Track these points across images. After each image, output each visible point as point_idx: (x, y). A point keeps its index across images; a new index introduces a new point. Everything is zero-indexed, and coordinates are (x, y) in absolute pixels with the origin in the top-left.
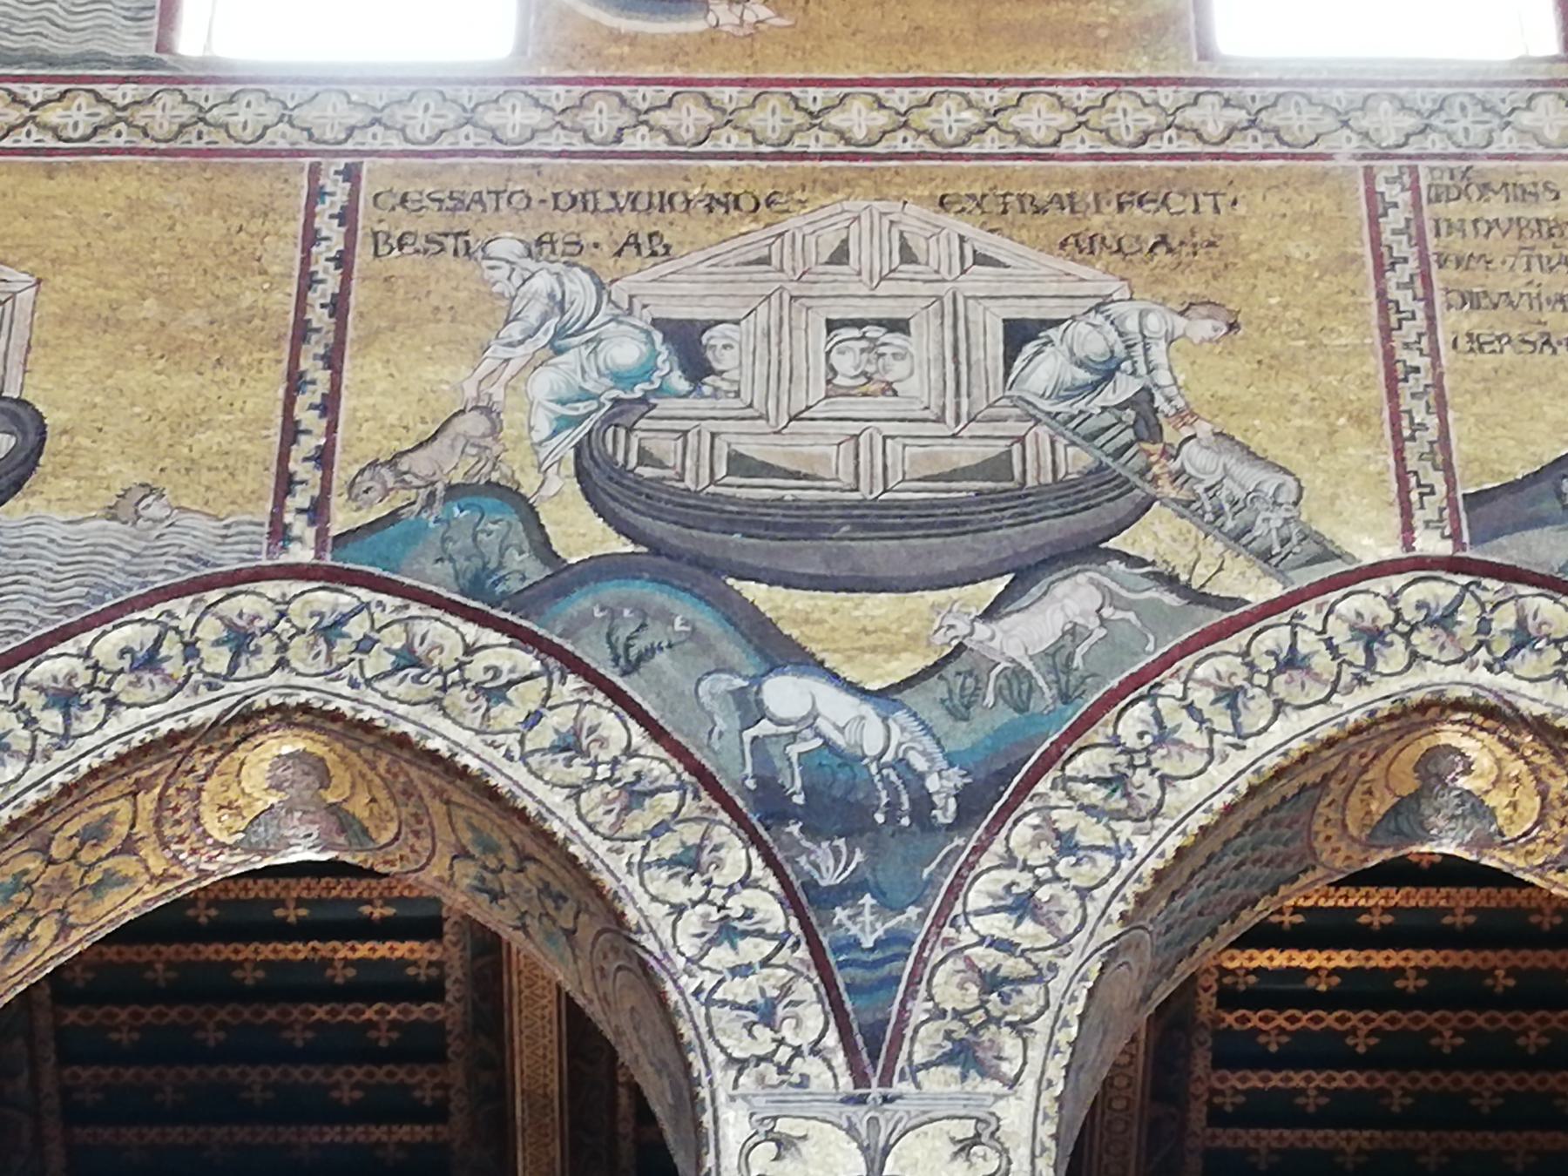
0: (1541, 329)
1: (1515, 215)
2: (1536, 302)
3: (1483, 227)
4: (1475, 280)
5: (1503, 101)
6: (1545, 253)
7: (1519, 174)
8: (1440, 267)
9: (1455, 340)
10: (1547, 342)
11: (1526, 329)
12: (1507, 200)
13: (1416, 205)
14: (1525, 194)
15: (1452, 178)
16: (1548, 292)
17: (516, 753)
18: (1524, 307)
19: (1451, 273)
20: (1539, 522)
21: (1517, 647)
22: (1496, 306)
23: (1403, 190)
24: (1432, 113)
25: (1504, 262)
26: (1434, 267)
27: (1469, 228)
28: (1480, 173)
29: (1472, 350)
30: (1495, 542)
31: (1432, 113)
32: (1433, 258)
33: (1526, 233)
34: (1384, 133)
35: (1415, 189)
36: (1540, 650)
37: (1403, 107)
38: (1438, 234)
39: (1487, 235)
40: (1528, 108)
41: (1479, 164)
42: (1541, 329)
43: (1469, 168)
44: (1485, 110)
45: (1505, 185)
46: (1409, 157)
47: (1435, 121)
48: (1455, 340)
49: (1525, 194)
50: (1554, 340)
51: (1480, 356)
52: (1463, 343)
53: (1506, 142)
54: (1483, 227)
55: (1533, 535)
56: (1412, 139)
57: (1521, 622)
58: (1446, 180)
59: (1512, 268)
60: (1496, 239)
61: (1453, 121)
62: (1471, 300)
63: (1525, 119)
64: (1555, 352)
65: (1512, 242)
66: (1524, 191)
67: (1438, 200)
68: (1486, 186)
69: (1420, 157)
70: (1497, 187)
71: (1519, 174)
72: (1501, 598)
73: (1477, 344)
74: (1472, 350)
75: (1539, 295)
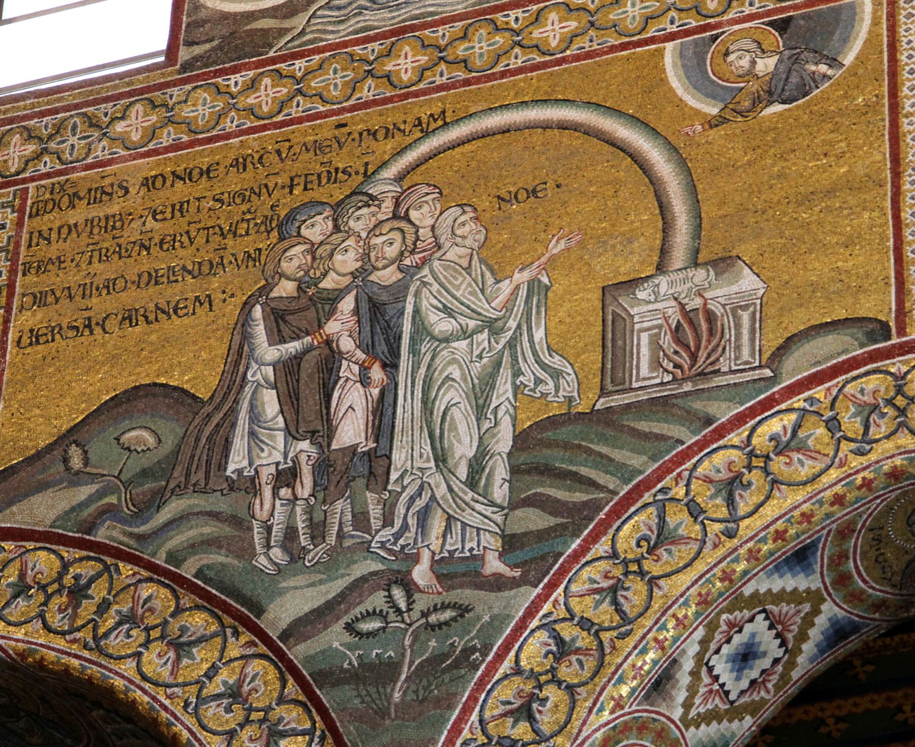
0: (86, 314)
1: (90, 217)
2: (86, 291)
3: (65, 230)
4: (54, 279)
5: (106, 114)
6: (106, 245)
7: (103, 177)
8: (24, 275)
9: (21, 337)
10: (89, 326)
11: (75, 317)
12: (89, 204)
13: (20, 224)
14: (100, 195)
15: (52, 193)
16: (99, 281)
17: (90, 640)
18: (78, 298)
19: (32, 278)
20: (42, 487)
21: (15, 596)
22: (57, 300)
23: (13, 212)
24: (50, 137)
25: (72, 261)
26: (20, 274)
27: (54, 236)
28: (74, 183)
29: (31, 344)
30: (8, 511)
31: (50, 137)
32: (20, 268)
33: (96, 231)
34: (10, 163)
35: (21, 211)
36: (32, 595)
37: (30, 135)
38: (30, 246)
39: (65, 240)
40: (123, 118)
41: (74, 176)
42: (86, 314)
43: (67, 180)
44: (91, 125)
45: (90, 190)
46: (24, 181)
47: (53, 145)
48: (21, 337)
49: (100, 195)
50: (93, 323)
51: (40, 347)
52: (25, 340)
53: (100, 152)
54: (65, 230)
55: (37, 499)
56: (30, 164)
57: (22, 575)
58: (47, 196)
59: (77, 265)
60: (72, 241)
61: (64, 142)
62: (39, 300)
63: (120, 127)
64: (91, 333)
65: (84, 239)
66: (104, 192)
67: (37, 214)
68: (75, 194)
69: (32, 179)
70: (82, 194)
71: (103, 177)
72: (12, 556)
73: (36, 337)
74: (31, 344)
75: (92, 283)
